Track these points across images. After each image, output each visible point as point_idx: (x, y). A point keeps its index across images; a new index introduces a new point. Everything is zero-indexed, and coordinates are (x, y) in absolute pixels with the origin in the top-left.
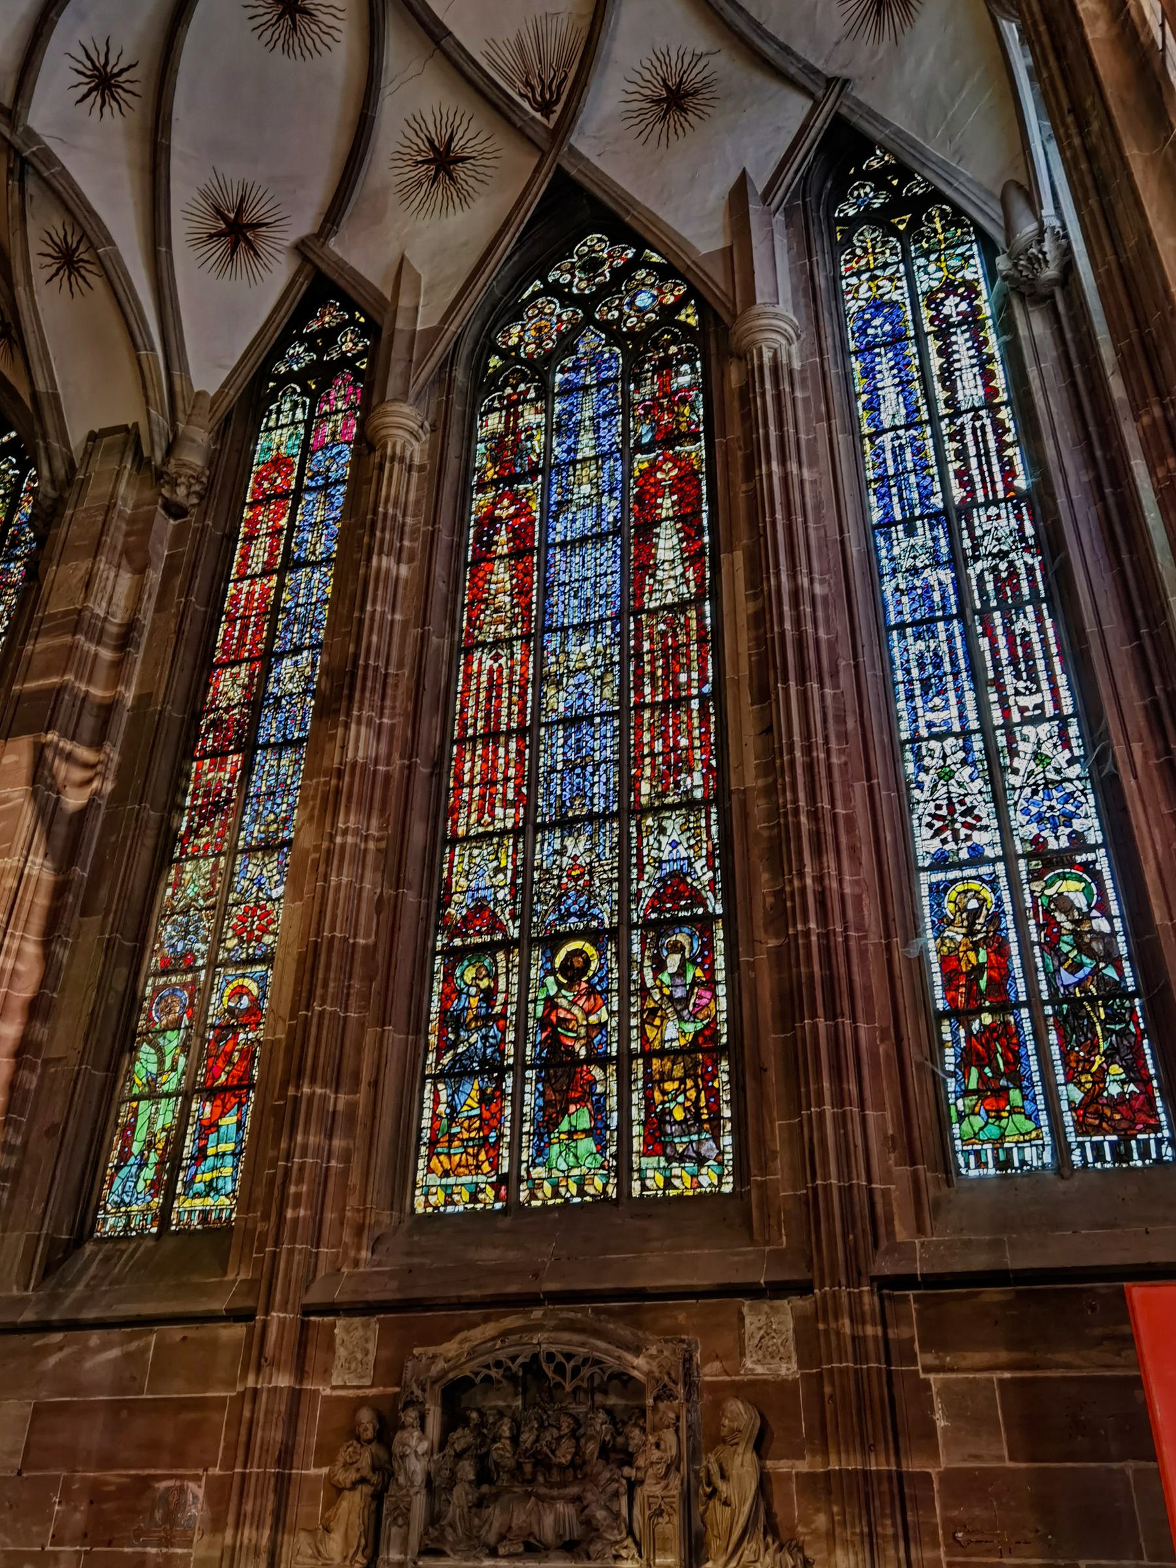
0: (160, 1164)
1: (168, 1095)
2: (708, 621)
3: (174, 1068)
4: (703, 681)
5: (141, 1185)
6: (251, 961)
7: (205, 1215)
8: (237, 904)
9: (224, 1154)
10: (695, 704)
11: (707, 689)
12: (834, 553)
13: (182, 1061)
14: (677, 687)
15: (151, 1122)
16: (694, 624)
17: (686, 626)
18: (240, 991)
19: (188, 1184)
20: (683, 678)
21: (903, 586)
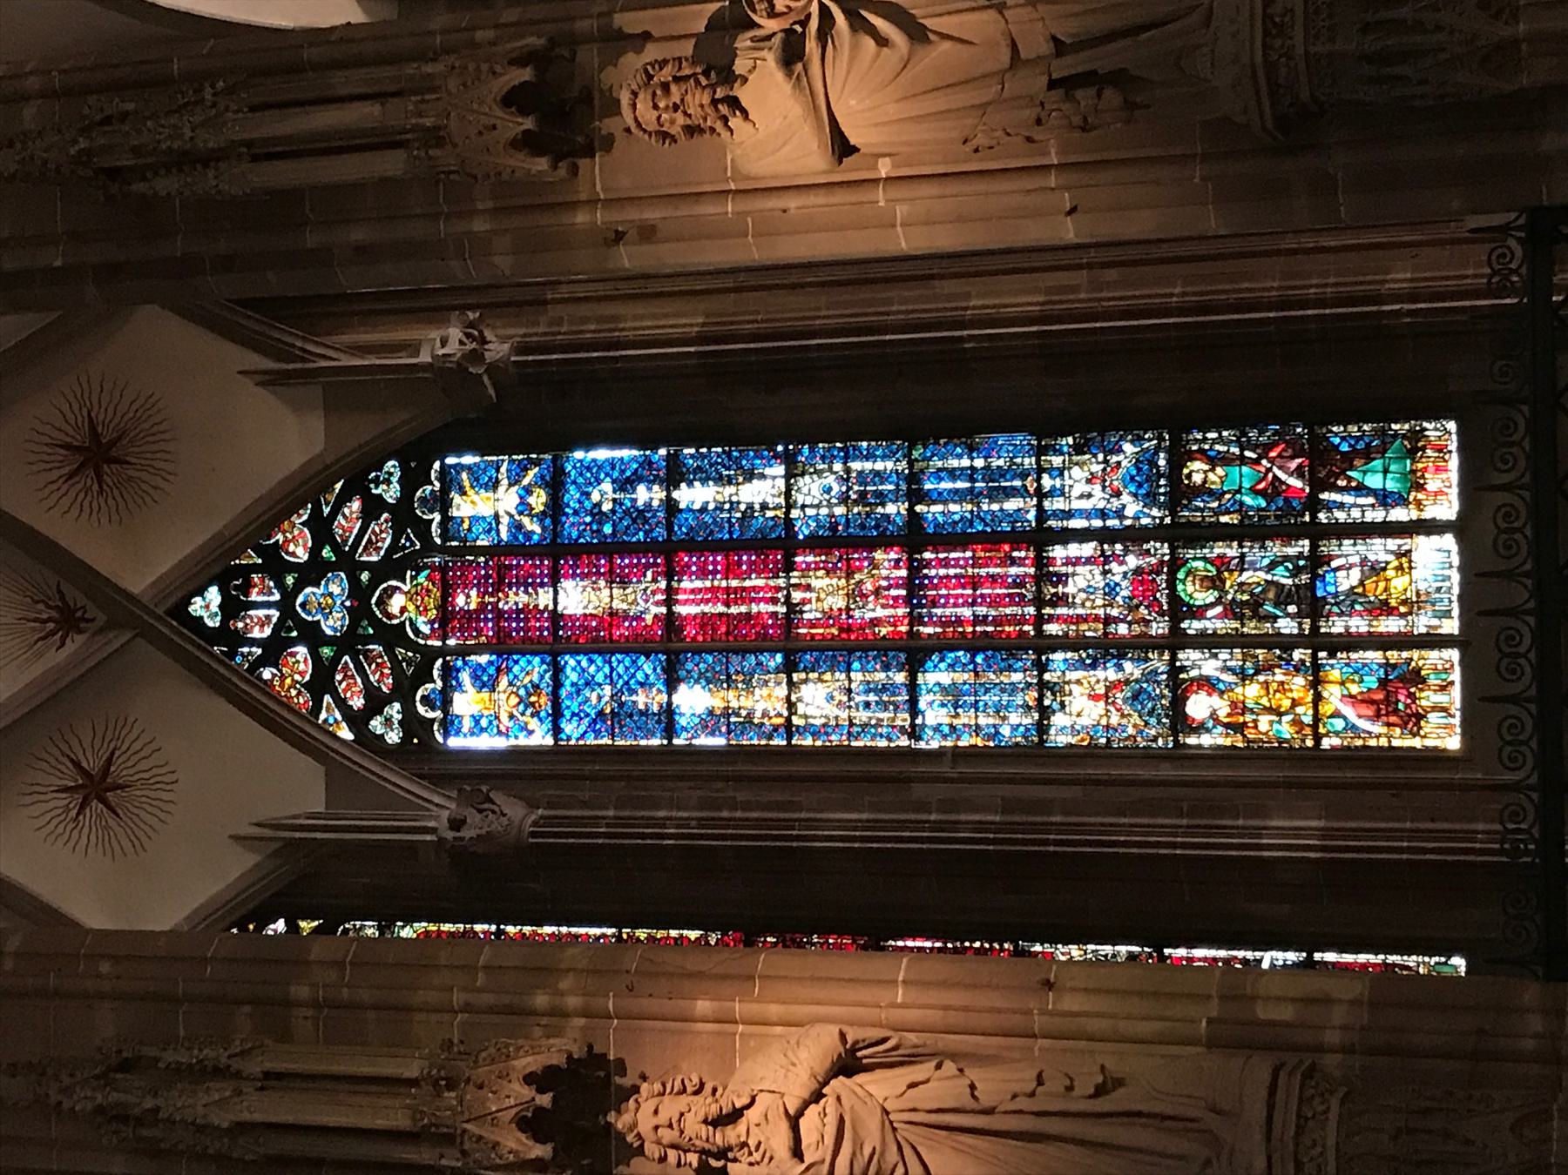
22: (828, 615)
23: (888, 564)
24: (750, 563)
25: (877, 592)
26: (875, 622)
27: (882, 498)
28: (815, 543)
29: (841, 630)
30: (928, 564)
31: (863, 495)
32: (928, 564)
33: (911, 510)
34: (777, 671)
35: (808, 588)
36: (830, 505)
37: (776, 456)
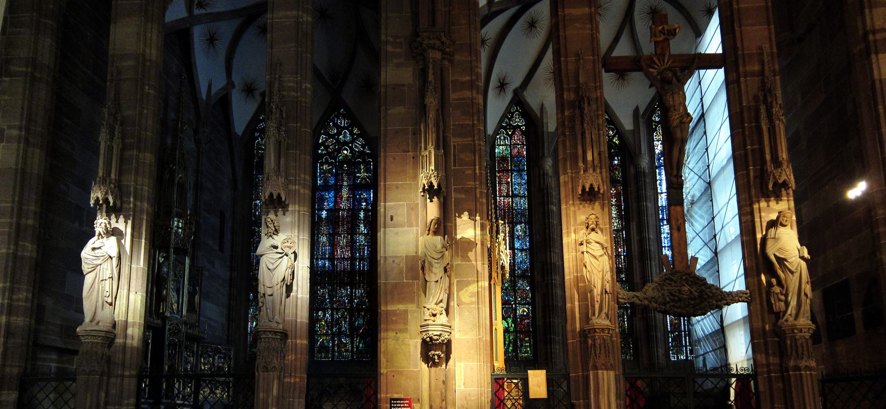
0: (513, 347)
1: (511, 332)
2: (624, 236)
3: (512, 326)
4: (624, 252)
5: (510, 351)
6: (524, 304)
7: (525, 357)
8: (518, 289)
9: (527, 346)
10: (622, 257)
11: (625, 254)
12: (655, 229)
13: (513, 325)
14: (619, 252)
15: (509, 338)
16: (621, 236)
17: (620, 236)
18: (524, 311)
19: (521, 351)
20: (620, 250)
21: (666, 237)
22: (339, 242)
23: (348, 254)
24: (349, 226)
25: (343, 252)
26: (337, 252)
27: (360, 253)
28: (352, 238)
29: (336, 245)
30: (348, 262)
31: (361, 249)
32: (348, 262)
33: (358, 258)
34: (329, 232)
35: (344, 238)
36: (359, 242)
37: (369, 232)
